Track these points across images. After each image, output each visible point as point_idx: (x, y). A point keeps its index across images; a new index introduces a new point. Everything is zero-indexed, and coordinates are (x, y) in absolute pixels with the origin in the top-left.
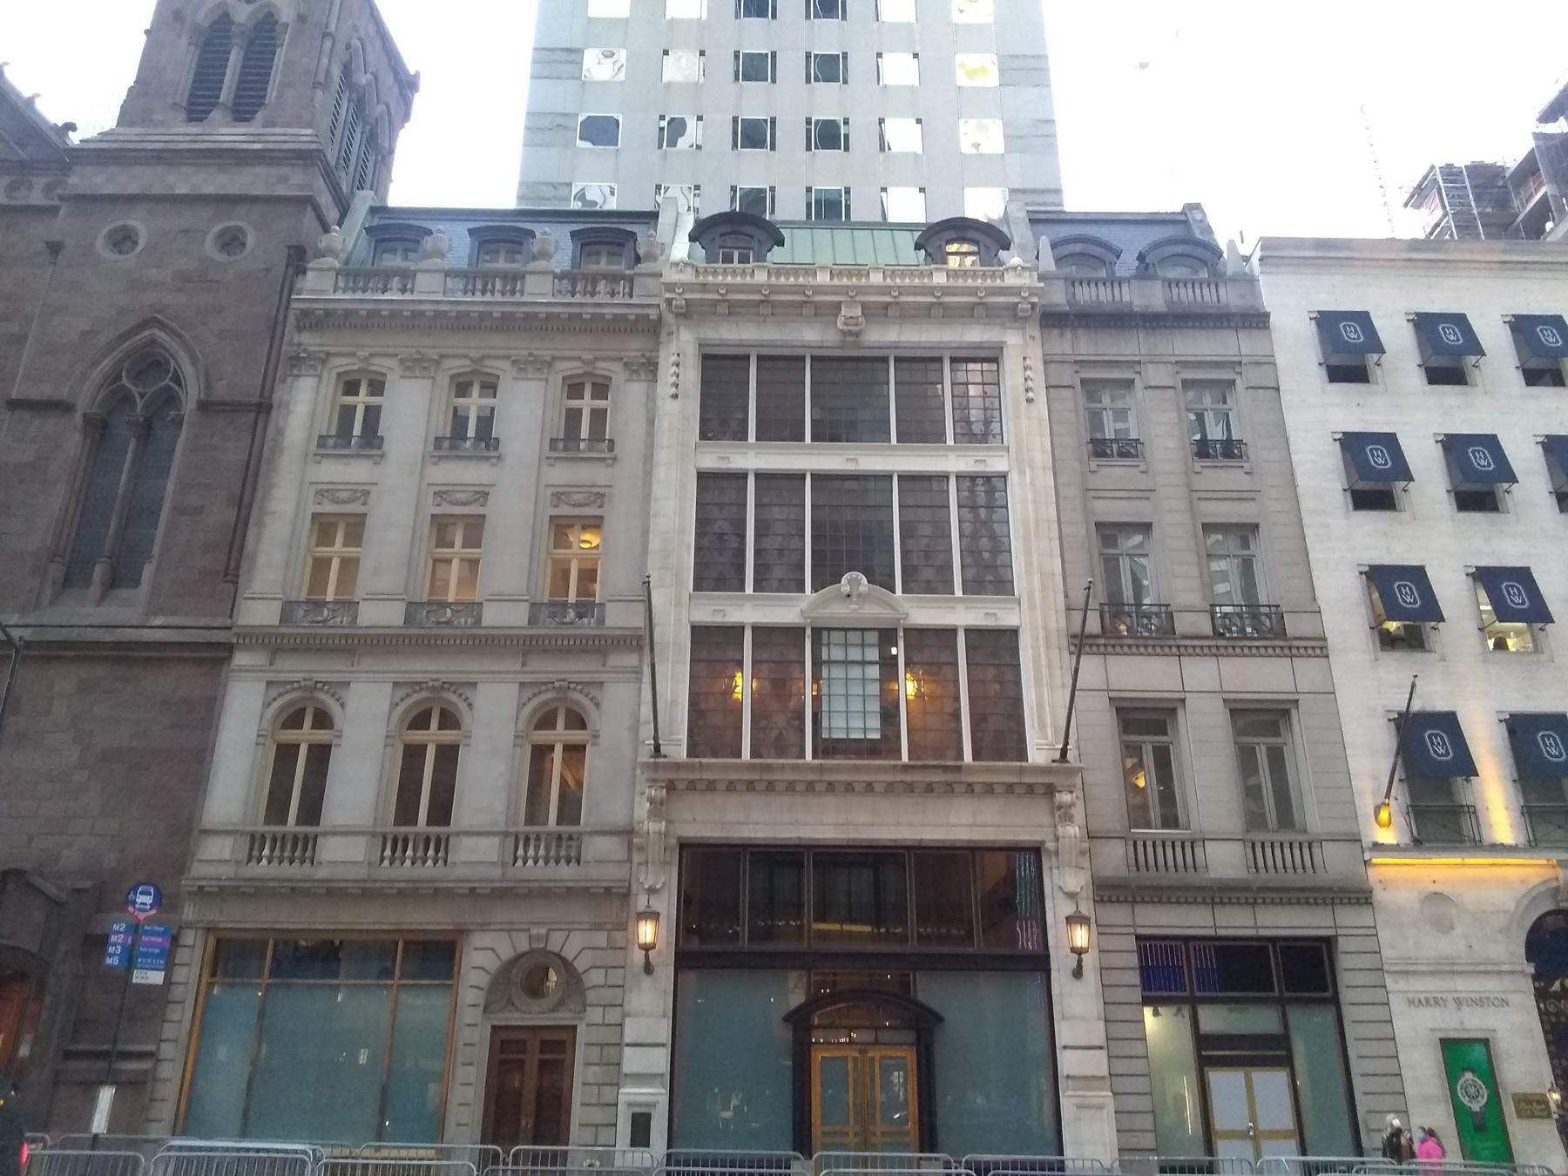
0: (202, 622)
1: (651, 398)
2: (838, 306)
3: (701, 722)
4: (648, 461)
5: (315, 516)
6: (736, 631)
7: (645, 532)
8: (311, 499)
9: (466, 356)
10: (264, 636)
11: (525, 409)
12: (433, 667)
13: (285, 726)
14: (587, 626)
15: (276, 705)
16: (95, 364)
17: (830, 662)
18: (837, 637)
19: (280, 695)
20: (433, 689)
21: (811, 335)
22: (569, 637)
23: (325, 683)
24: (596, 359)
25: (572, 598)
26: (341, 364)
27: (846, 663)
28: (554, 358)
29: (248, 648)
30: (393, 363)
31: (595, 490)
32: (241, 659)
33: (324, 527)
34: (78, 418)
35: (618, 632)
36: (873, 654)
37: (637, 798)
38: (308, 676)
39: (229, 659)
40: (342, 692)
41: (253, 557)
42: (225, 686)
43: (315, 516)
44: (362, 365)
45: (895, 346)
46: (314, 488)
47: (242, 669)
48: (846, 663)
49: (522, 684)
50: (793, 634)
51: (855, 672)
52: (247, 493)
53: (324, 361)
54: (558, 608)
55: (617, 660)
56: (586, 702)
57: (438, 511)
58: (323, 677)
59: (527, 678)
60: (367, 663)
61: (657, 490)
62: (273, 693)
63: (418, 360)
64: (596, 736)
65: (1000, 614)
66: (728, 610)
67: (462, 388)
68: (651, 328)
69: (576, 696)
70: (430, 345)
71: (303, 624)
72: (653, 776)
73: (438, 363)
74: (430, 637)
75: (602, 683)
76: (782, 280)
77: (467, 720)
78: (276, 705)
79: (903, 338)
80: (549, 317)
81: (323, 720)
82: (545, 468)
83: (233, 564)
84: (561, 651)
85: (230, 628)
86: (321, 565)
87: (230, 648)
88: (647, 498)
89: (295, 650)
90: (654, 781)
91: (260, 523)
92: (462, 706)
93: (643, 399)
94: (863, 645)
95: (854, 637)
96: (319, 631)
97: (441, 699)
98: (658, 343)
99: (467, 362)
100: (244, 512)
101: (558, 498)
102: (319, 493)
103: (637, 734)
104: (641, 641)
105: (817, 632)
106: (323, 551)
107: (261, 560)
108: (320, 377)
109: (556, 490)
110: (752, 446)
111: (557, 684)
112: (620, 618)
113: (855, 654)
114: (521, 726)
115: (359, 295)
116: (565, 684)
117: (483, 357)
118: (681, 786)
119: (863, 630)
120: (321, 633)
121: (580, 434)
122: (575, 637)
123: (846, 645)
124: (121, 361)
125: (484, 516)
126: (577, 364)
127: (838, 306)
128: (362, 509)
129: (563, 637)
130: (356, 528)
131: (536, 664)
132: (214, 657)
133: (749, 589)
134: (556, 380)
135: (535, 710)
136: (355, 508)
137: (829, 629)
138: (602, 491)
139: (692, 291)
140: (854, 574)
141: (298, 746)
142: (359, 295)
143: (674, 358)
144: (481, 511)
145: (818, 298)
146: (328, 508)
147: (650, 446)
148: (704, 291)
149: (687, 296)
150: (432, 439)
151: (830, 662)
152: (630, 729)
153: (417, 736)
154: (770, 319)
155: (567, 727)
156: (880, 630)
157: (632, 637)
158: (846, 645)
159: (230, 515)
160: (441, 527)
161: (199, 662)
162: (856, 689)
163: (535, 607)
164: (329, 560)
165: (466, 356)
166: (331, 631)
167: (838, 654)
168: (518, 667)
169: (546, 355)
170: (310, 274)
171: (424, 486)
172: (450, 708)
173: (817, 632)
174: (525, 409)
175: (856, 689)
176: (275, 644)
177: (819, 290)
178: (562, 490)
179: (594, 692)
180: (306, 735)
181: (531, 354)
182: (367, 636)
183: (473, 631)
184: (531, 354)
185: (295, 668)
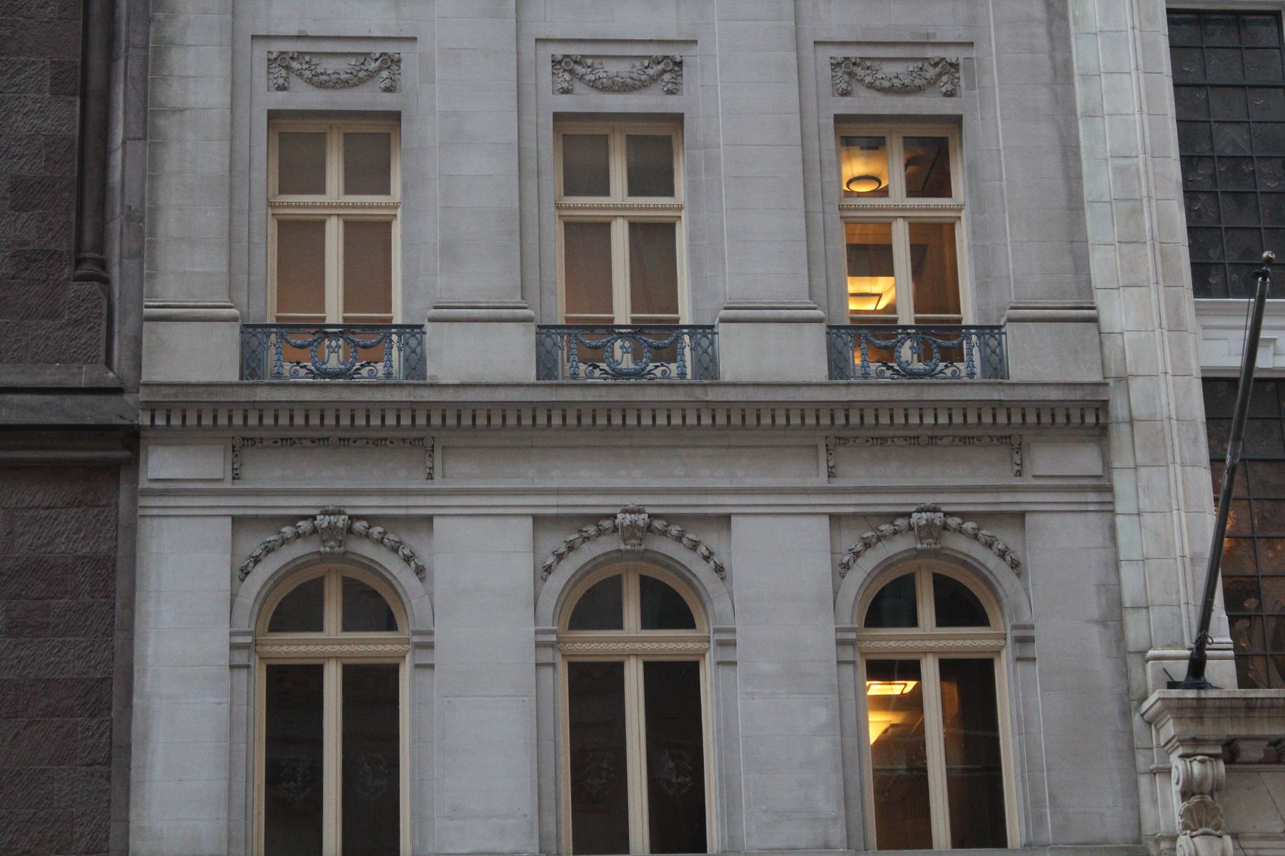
0: (50, 376)
3: (1250, 604)
5: (274, 116)
7: (1070, 151)
8: (261, 69)
10: (215, 408)
12: (639, 478)
13: (278, 624)
14: (963, 381)
15: (261, 575)
19: (269, 550)
20: (632, 532)
22: (935, 407)
23: (372, 520)
25: (622, 313)
29: (178, 437)
32: (161, 464)
33: (296, 145)
35: (1054, 395)
37: (1144, 781)
38: (331, 502)
39: (133, 464)
40: (413, 542)
41: (143, 222)
42: (133, 529)
43: (274, 116)
46: (261, 51)
47: (170, 490)
49: (835, 519)
52: (96, 59)
54: (591, 334)
55: (1048, 460)
56: (989, 560)
57: (280, 101)
58: (368, 505)
59: (847, 504)
60: (460, 471)
61: (1083, 53)
62: (252, 544)
64: (1025, 641)
69: (962, 545)
71: (292, 378)
72: (1193, 730)
74: (609, 409)
75: (1022, 515)
77: (717, 606)
78: (261, 575)
81: (372, 607)
83: (89, 237)
84: (914, 440)
85: (119, 391)
86: (300, 238)
87: (130, 440)
88: (1062, 72)
89: (287, 442)
90: (1196, 742)
91: (147, 132)
92: (702, 571)
96: (332, 395)
97: (345, 557)
100: (94, 106)
101: (849, 70)
102: (279, 61)
103: (1120, 636)
104: (1086, 416)
106: (301, 203)
107: (169, 224)
109: (840, 53)
111: (920, 519)
112: (1036, 361)
114: (244, 624)
116: (938, 518)
118: (1251, 752)
120: (339, 402)
122: (950, 406)
125: (677, 120)
128: (386, 102)
129: (921, 407)
130: (373, 144)
131: (856, 472)
132: (98, 457)
135: (276, 580)
136: (368, 98)
138: (951, 55)
141: (320, 669)
144: (671, 104)
146: (305, 97)
152: (1103, 622)
153: (294, 646)
155: (942, 620)
157: (1083, 406)
159: (63, 118)
160: (580, 149)
161: (58, 471)
163: (251, 330)
164: (318, 226)
166: (366, 395)
168: (821, 481)
171: (529, 46)
172: (656, 573)
176: (239, 425)
178: (854, 53)
179: (413, 542)
180: (333, 644)
182: (459, 408)
183: (699, 394)
185: (300, 485)
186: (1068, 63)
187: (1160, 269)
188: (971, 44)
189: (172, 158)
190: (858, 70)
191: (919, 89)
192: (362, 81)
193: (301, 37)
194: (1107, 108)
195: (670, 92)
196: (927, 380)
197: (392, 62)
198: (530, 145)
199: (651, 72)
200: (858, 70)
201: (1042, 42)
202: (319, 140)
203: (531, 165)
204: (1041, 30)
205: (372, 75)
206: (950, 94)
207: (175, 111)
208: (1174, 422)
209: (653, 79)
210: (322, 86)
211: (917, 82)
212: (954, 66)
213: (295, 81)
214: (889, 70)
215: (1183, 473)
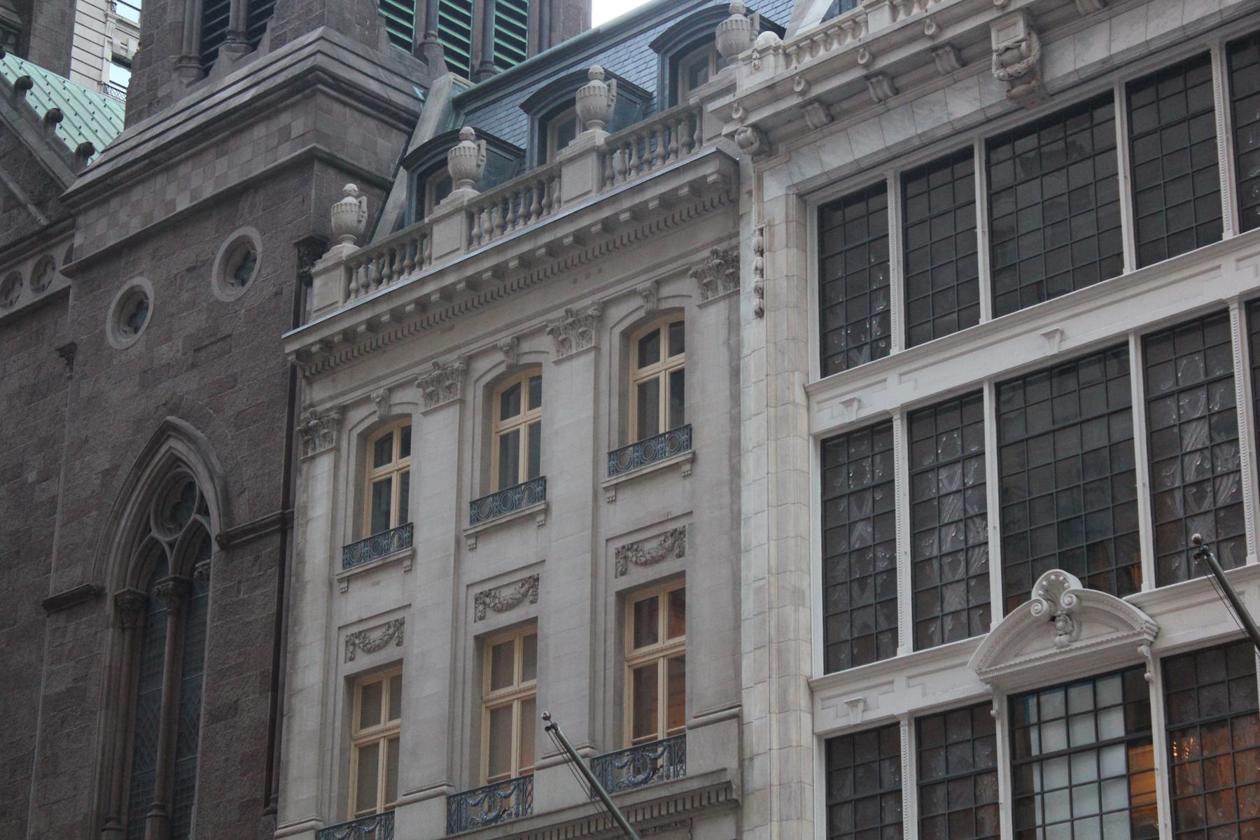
1: (734, 325)
2: (984, 33)
4: (735, 446)
5: (351, 680)
6: (885, 733)
9: (633, 293)
11: (574, 410)
16: (118, 516)
17: (1044, 759)
18: (1053, 704)
21: (962, 105)
24: (659, 283)
26: (361, 418)
27: (1071, 754)
28: (604, 306)
30: (413, 394)
31: (671, 527)
34: (109, 608)
36: (1115, 726)
44: (649, 306)
45: (1108, 68)
48: (1071, 754)
50: (973, 714)
51: (1086, 770)
53: (340, 423)
63: (438, 380)
65: (1166, 622)
66: (871, 696)
67: (644, 346)
68: (724, 194)
70: (446, 347)
73: (466, 372)
76: (916, 12)
79: (1119, 46)
80: (667, 201)
82: (605, 509)
88: (736, 518)
93: (723, 335)
94: (1096, 712)
95: (1081, 699)
98: (738, 218)
99: (500, 356)
105: (1016, 702)
108: (597, 349)
109: (619, 544)
110: (1233, 246)
113: (1084, 734)
115: (534, 224)
117: (519, 339)
119: (1066, 686)
121: (653, 436)
123: (1068, 719)
124: (144, 505)
126: (637, 302)
127: (984, 33)
133: (905, 647)
134: (611, 341)
137: (1038, 692)
139: (761, 106)
140: (1054, 573)
142: (534, 224)
143: (755, 240)
145: (950, 33)
146: (364, 662)
147: (736, 421)
148: (777, 98)
149: (753, 119)
150: (466, 506)
151: (1044, 759)
154: (893, 102)
156: (1121, 672)
158: (1068, 719)
162: (1088, 805)
165: (633, 293)
167: (1054, 739)
169: (453, 361)
170: (317, 282)
171: (463, 589)
173: (1016, 702)
174: (574, 410)
175: (1088, 805)
177: (878, 47)
181: (569, 312)
184: (569, 312)
186: (739, 511)
187: (774, 665)
188: (691, 513)
189: (296, 726)
190: (630, 554)
191: (662, 558)
192: (387, 643)
193: (360, 621)
194: (754, 543)
195: (532, 602)
196: (643, 786)
197: (400, 623)
198: (460, 664)
199: (522, 591)
200: (630, 554)
201: (726, 500)
202: (654, 602)
203: (460, 678)
204: (726, 489)
205: (391, 637)
206: (680, 556)
207: (301, 691)
208: (775, 789)
209: (525, 595)
210: (369, 651)
211: (660, 552)
212: (682, 533)
213: (359, 652)
214: (648, 546)
215: (780, 826)
